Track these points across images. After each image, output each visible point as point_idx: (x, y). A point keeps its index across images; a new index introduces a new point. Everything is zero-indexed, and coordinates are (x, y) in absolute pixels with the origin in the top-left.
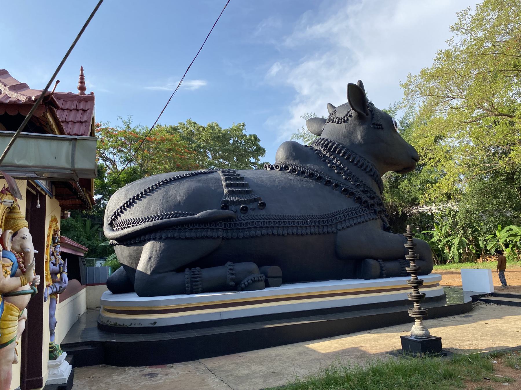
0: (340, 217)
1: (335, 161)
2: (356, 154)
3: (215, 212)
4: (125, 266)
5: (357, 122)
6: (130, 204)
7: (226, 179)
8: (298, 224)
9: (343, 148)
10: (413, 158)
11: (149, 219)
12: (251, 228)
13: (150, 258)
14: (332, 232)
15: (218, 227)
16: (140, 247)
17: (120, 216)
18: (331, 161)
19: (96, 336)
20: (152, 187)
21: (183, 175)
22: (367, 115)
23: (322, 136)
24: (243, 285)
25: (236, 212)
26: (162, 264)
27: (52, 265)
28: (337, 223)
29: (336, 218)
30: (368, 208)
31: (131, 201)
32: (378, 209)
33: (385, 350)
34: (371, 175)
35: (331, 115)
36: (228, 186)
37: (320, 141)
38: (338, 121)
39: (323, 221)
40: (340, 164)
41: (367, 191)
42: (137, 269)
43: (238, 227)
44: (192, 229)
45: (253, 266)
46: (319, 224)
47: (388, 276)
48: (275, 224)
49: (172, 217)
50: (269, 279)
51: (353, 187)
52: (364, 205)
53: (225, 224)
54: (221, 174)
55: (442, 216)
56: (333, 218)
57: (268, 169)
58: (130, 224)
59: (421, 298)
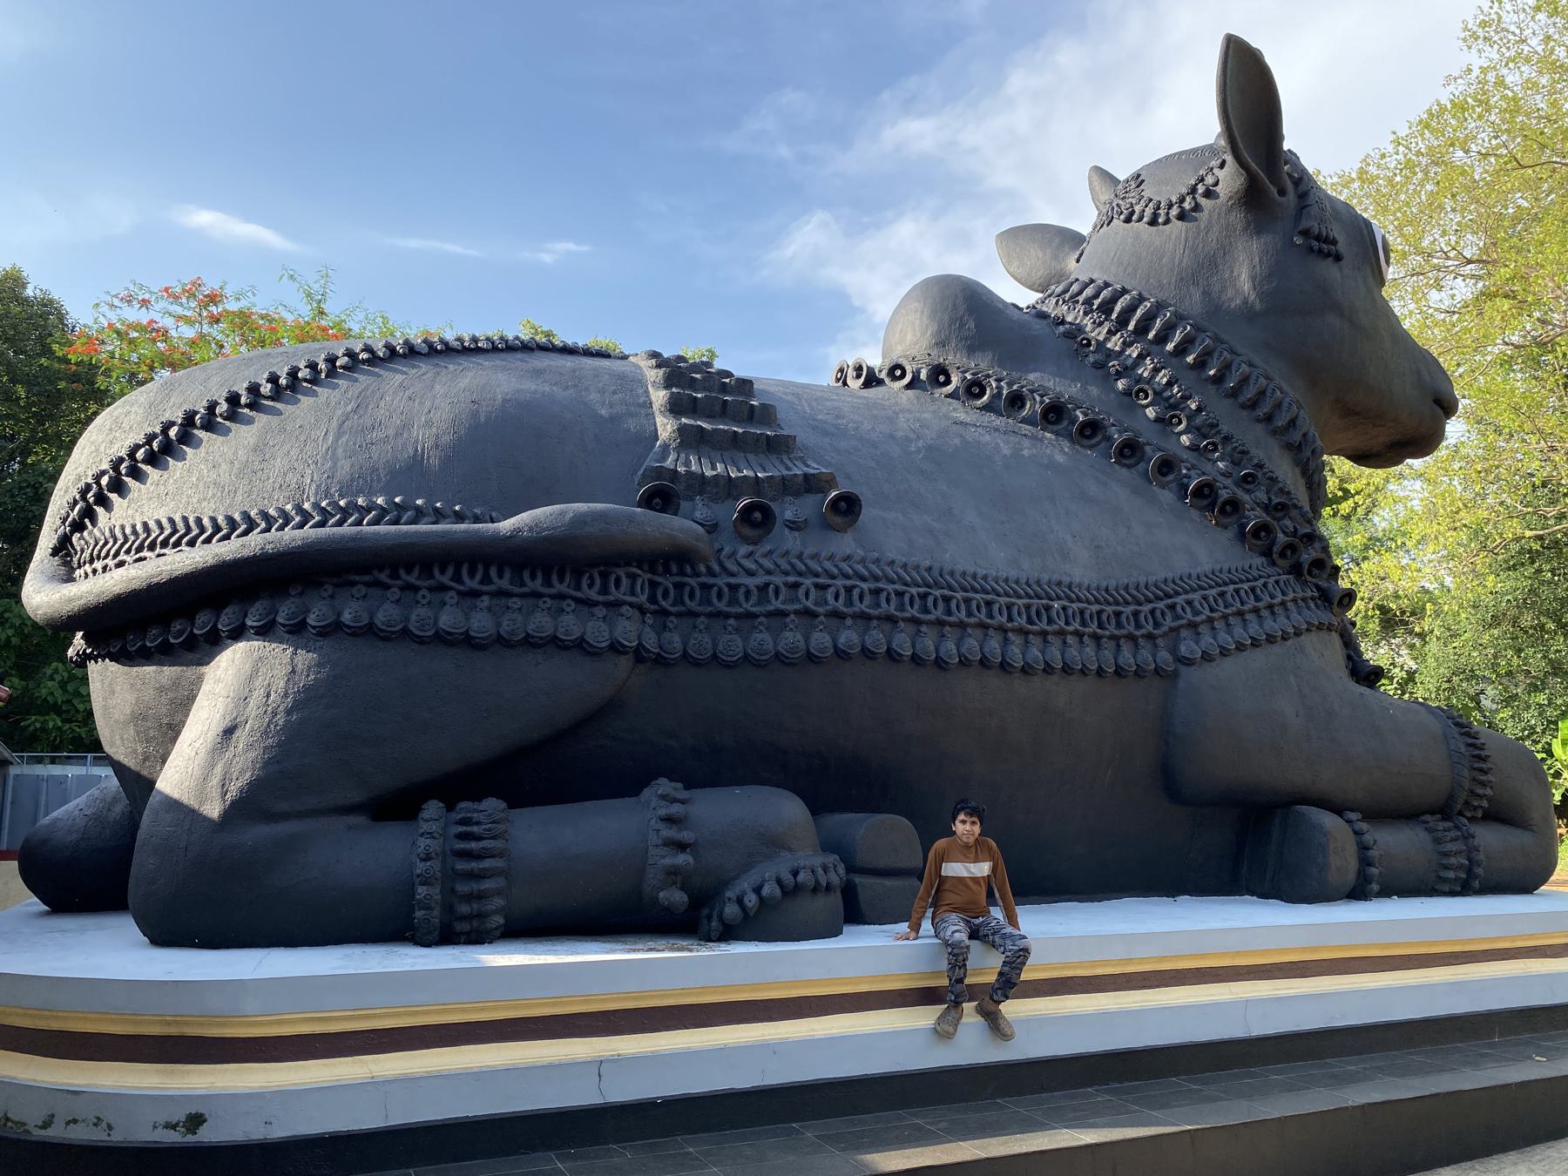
1: (1144, 371)
4: (120, 769)
5: (1238, 218)
6: (162, 449)
8: (1010, 619)
9: (1179, 318)
12: (784, 614)
13: (229, 732)
15: (614, 595)
16: (190, 672)
18: (1127, 371)
20: (293, 373)
22: (1282, 192)
24: (731, 910)
25: (712, 528)
29: (1172, 607)
31: (173, 432)
34: (1289, 446)
38: (1155, 216)
39: (1118, 614)
40: (1170, 384)
43: (722, 606)
44: (475, 594)
45: (788, 810)
46: (1100, 626)
47: (1387, 892)
48: (901, 608)
49: (376, 522)
51: (1228, 482)
52: (1279, 561)
56: (1161, 605)
57: (855, 384)
58: (152, 547)
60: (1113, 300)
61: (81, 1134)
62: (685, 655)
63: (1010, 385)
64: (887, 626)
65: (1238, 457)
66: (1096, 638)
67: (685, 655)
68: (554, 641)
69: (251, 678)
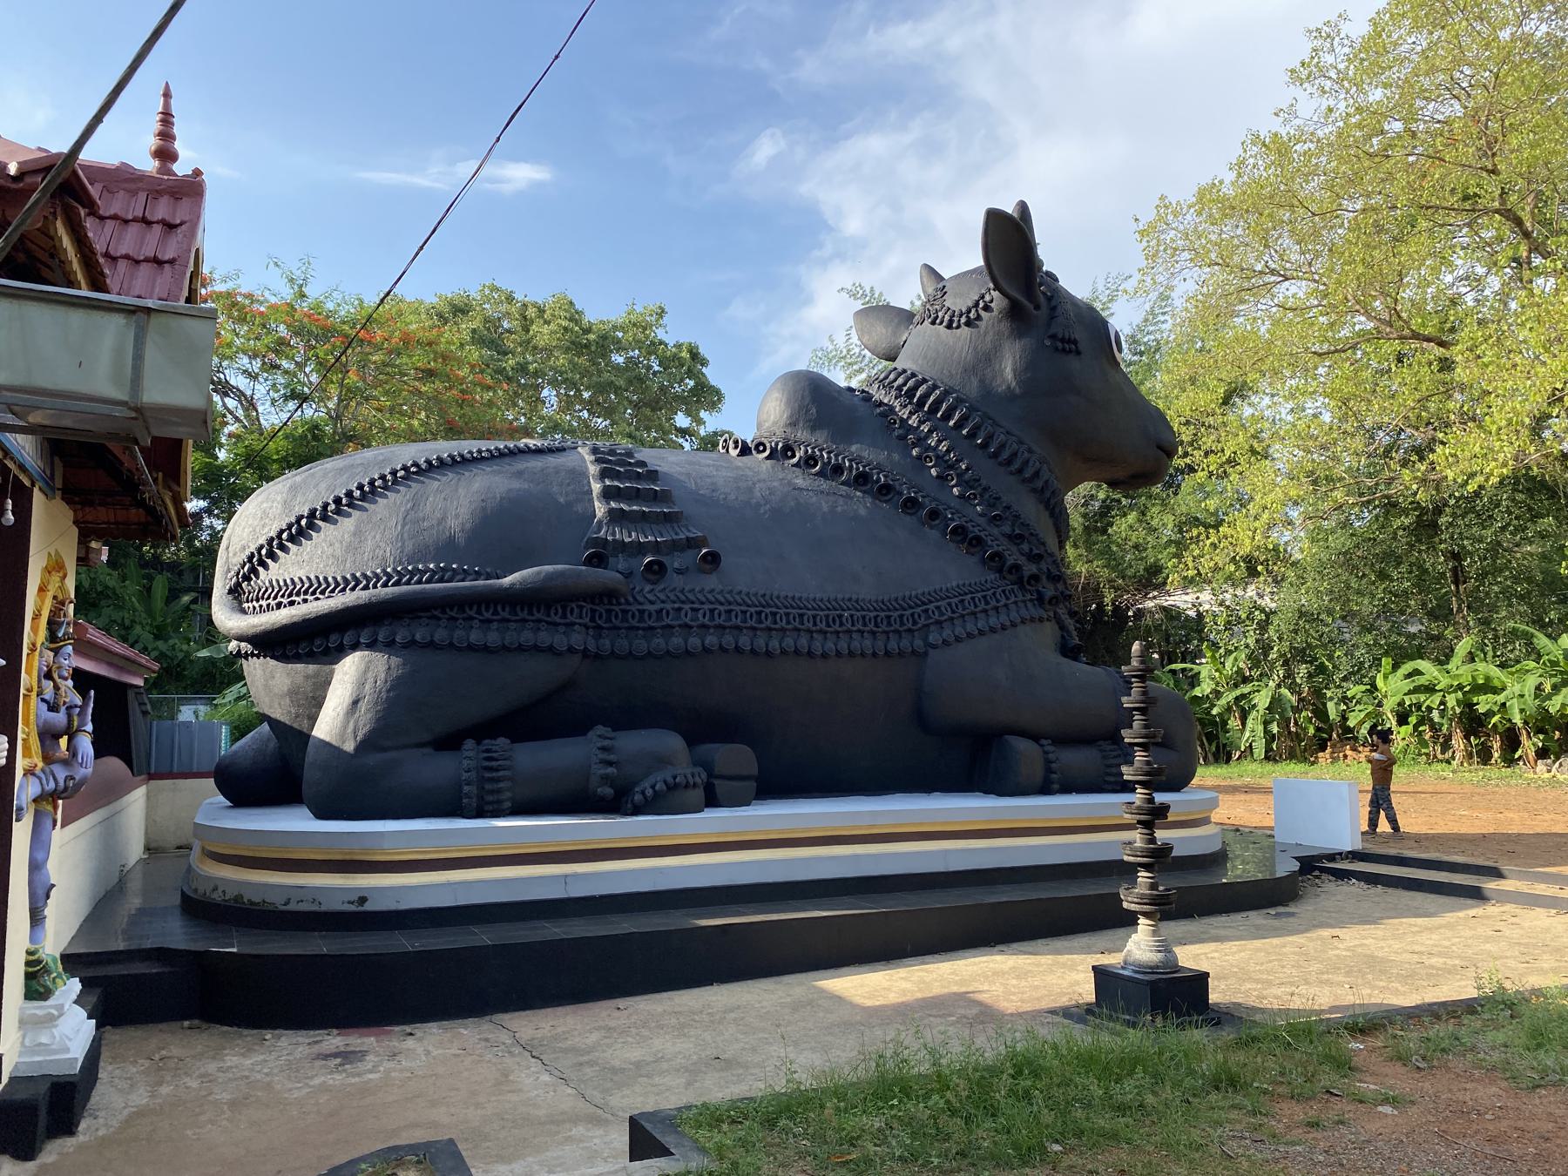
0: (938, 608)
2: (995, 423)
3: (562, 574)
4: (274, 723)
5: (1005, 326)
6: (299, 531)
7: (603, 475)
8: (815, 624)
9: (959, 401)
10: (1159, 447)
11: (358, 583)
12: (672, 627)
13: (355, 703)
14: (914, 652)
15: (571, 619)
16: (327, 668)
17: (266, 567)
18: (921, 441)
19: (176, 934)
20: (372, 483)
21: (471, 452)
22: (1037, 307)
23: (900, 364)
24: (638, 798)
25: (628, 575)
26: (392, 723)
27: (45, 707)
28: (927, 626)
29: (926, 611)
30: (1022, 588)
31: (303, 522)
32: (1049, 592)
33: (1046, 1004)
34: (1034, 490)
35: (931, 300)
36: (607, 494)
37: (892, 377)
38: (951, 321)
39: (889, 617)
40: (948, 451)
41: (1021, 537)
42: (314, 733)
43: (635, 623)
44: (490, 621)
45: (672, 742)
46: (876, 625)
47: (1067, 789)
49: (428, 582)
50: (716, 782)
51: (982, 521)
53: (593, 611)
54: (589, 458)
55: (1229, 622)
56: (918, 610)
57: (734, 453)
58: (298, 594)
59: (1159, 858)
60: (916, 388)
61: (305, 907)
62: (613, 652)
63: (837, 456)
64: (736, 632)
65: (993, 502)
66: (873, 633)
67: (613, 652)
68: (536, 648)
69: (365, 672)
